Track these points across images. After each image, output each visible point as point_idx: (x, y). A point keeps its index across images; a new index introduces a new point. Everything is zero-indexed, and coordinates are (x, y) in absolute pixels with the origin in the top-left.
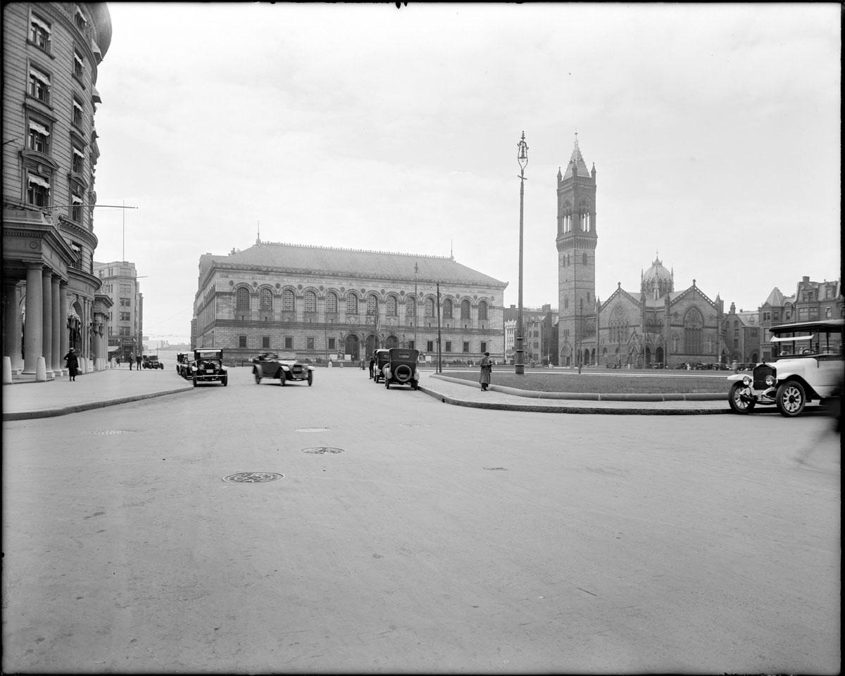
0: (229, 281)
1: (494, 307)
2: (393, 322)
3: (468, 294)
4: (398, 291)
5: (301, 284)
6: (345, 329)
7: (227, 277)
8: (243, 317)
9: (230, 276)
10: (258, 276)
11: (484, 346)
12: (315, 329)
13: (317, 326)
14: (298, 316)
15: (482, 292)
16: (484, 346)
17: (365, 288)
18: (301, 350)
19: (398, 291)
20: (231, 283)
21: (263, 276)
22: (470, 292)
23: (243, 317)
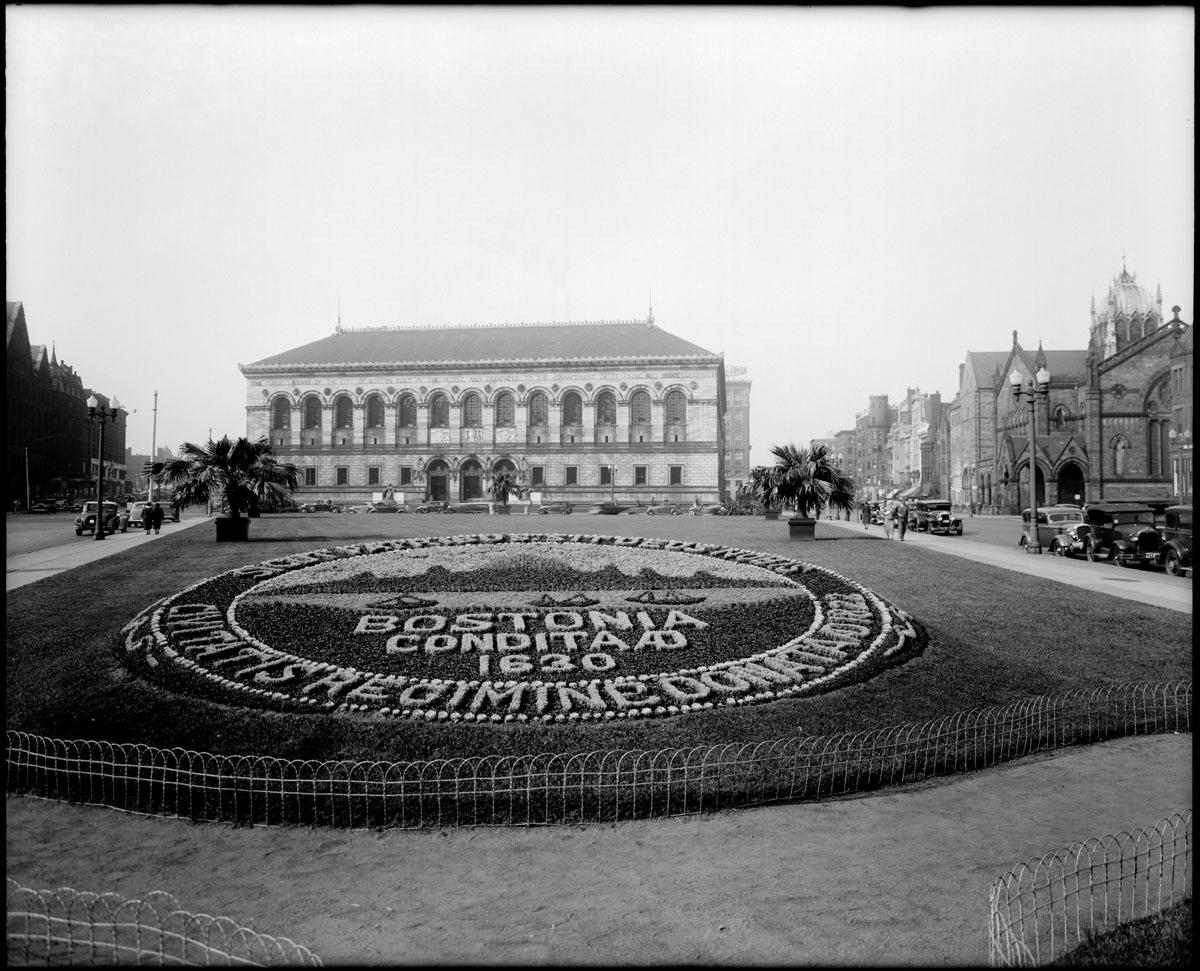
0: (262, 391)
1: (697, 402)
2: (504, 436)
3: (644, 382)
4: (514, 386)
5: (360, 386)
6: (427, 453)
7: (260, 385)
8: (282, 441)
9: (264, 382)
10: (300, 380)
11: (676, 473)
12: (380, 453)
13: (383, 450)
14: (355, 435)
15: (672, 376)
16: (676, 473)
17: (458, 384)
18: (360, 487)
19: (514, 386)
20: (266, 393)
21: (307, 379)
22: (648, 377)
23: (282, 441)
